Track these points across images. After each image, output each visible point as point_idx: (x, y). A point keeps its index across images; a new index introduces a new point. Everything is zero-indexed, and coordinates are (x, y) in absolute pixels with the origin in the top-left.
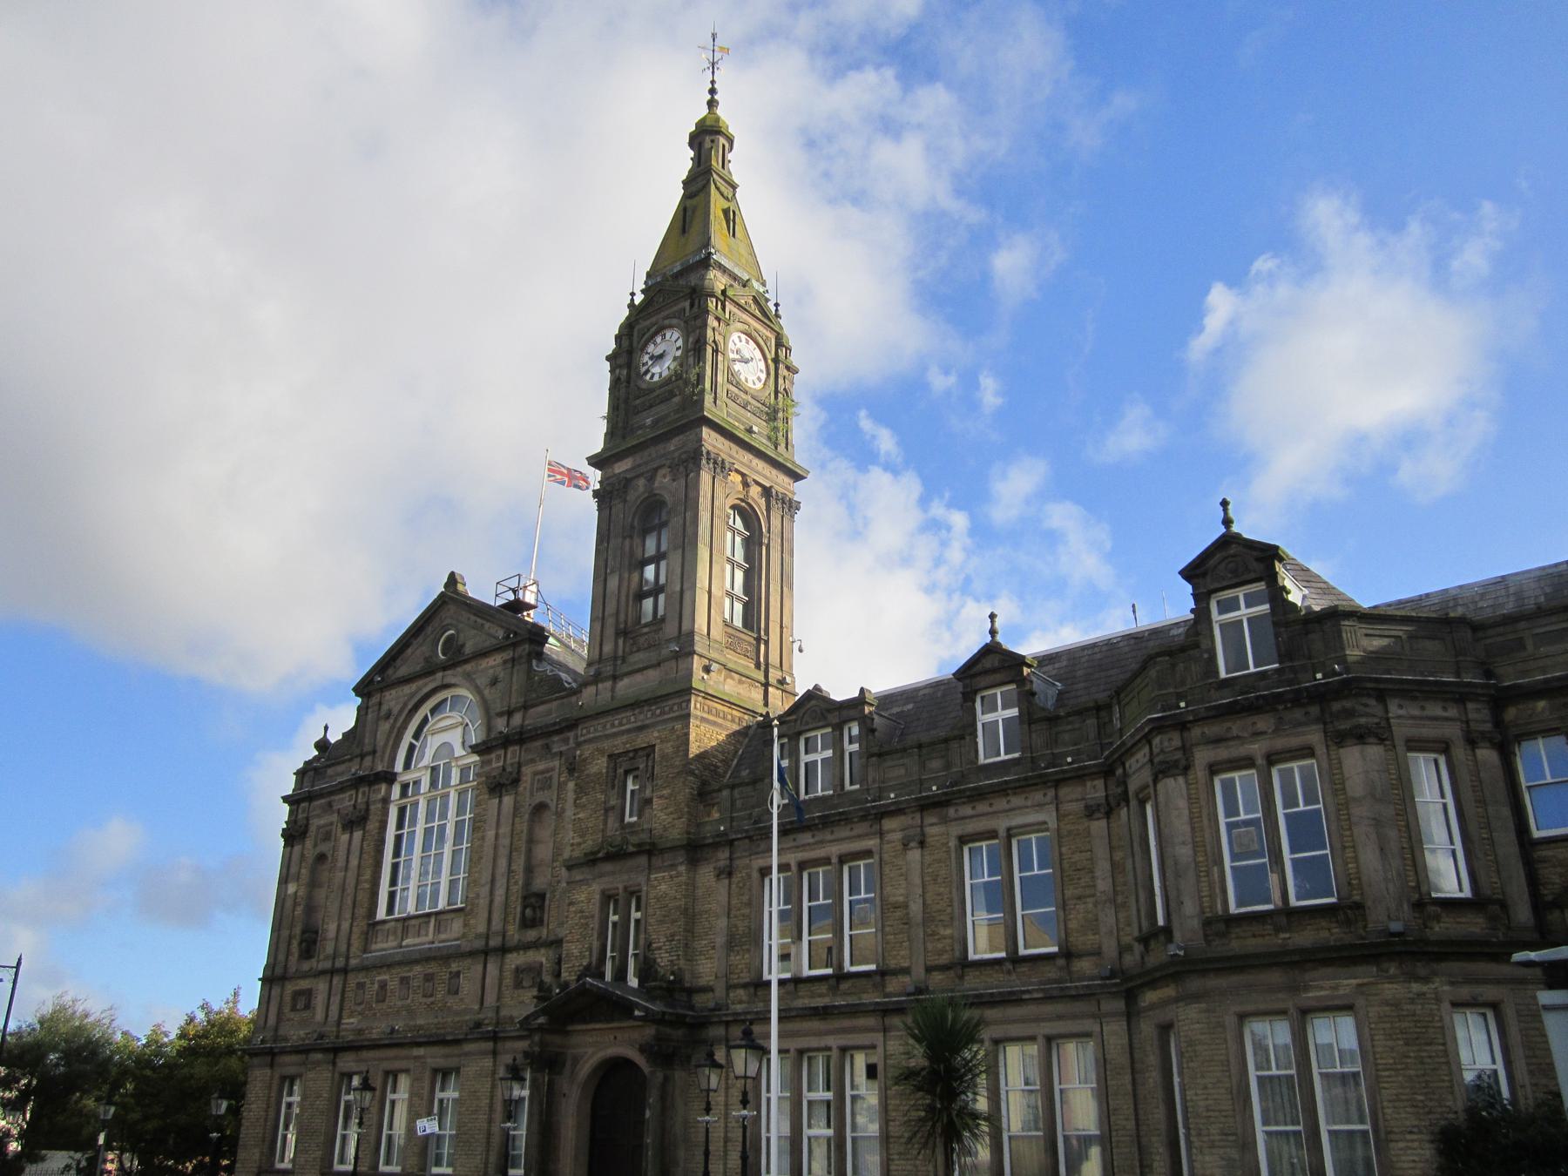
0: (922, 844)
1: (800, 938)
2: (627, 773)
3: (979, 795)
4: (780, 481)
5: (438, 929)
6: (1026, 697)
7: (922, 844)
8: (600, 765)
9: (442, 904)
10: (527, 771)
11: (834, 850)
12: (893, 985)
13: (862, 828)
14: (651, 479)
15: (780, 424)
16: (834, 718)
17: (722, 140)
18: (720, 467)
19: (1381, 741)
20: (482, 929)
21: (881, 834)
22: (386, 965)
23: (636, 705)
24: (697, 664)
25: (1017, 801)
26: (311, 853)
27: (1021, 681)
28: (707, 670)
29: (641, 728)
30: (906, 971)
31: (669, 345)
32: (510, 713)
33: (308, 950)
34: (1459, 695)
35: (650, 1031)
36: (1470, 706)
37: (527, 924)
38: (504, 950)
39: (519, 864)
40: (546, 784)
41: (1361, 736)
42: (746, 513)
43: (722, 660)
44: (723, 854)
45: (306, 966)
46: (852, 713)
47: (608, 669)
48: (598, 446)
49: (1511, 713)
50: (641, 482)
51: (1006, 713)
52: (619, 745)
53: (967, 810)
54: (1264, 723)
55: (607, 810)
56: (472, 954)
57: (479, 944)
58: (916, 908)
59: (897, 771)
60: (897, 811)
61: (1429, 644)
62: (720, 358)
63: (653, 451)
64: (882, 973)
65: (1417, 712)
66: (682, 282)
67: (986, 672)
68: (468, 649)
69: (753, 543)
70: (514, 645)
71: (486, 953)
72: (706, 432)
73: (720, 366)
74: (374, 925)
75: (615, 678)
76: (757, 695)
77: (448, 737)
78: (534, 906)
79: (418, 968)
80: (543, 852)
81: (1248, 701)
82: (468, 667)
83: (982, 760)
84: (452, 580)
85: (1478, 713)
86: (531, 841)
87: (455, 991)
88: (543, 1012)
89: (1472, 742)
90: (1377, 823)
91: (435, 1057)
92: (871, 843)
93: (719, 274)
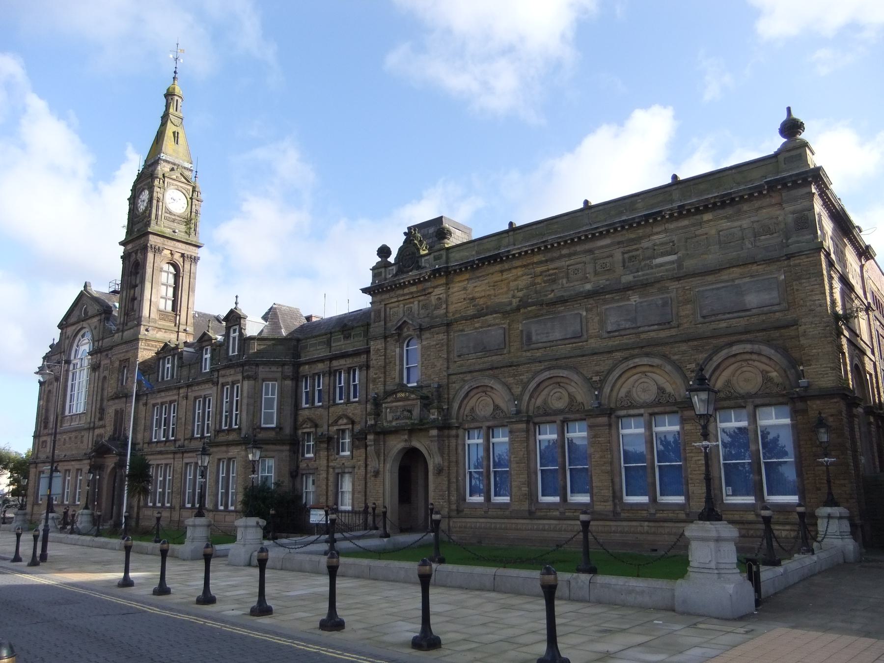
0: (187, 398)
1: (160, 427)
2: (124, 367)
3: (198, 384)
4: (190, 251)
5: (80, 420)
6: (213, 351)
7: (187, 398)
8: (117, 364)
9: (81, 410)
10: (102, 363)
11: (168, 399)
12: (178, 443)
13: (175, 392)
14: (136, 254)
15: (193, 226)
16: (172, 353)
17: (176, 98)
18: (158, 250)
19: (255, 379)
20: (89, 420)
21: (179, 394)
22: (65, 432)
23: (126, 343)
24: (142, 329)
25: (207, 386)
26: (47, 389)
27: (212, 345)
28: (147, 330)
29: (127, 352)
30: (179, 440)
31: (145, 195)
32: (98, 341)
33: (46, 427)
34: (283, 364)
35: (118, 458)
36: (286, 367)
37: (101, 419)
38: (94, 428)
39: (99, 398)
40: (106, 369)
41: (248, 378)
42: (175, 266)
43: (157, 325)
44: (145, 398)
45: (46, 431)
46: (176, 352)
47: (121, 328)
48: (123, 237)
49: (301, 368)
50: (134, 254)
51: (208, 356)
52: (122, 357)
53: (196, 388)
54: (232, 371)
55: (118, 380)
56: (85, 429)
57: (87, 426)
58: (183, 419)
59: (185, 372)
60: (182, 387)
61: (279, 347)
62: (161, 204)
63: (137, 242)
64: (175, 440)
65: (267, 369)
66: (150, 169)
67: (205, 341)
68: (89, 314)
69: (177, 276)
70: (100, 314)
71: (89, 429)
72: (151, 236)
73: (160, 207)
74: (64, 416)
75: (123, 331)
76: (173, 337)
77: (84, 347)
78: (102, 411)
79: (73, 435)
80: (105, 394)
81: (232, 364)
82: (89, 321)
83: (204, 371)
84: (85, 286)
85: (288, 370)
86: (103, 389)
87: (82, 442)
88: (94, 451)
89: (284, 378)
90: (248, 405)
91: (76, 465)
92: (176, 397)
93: (165, 164)
